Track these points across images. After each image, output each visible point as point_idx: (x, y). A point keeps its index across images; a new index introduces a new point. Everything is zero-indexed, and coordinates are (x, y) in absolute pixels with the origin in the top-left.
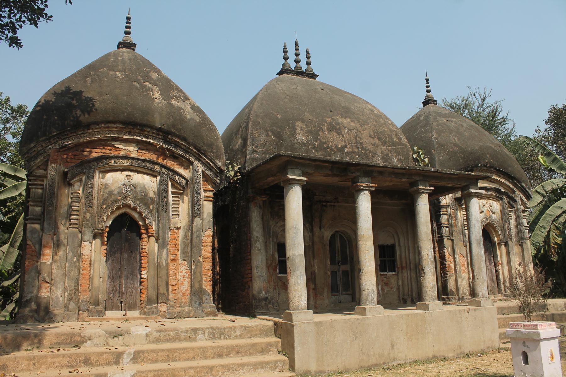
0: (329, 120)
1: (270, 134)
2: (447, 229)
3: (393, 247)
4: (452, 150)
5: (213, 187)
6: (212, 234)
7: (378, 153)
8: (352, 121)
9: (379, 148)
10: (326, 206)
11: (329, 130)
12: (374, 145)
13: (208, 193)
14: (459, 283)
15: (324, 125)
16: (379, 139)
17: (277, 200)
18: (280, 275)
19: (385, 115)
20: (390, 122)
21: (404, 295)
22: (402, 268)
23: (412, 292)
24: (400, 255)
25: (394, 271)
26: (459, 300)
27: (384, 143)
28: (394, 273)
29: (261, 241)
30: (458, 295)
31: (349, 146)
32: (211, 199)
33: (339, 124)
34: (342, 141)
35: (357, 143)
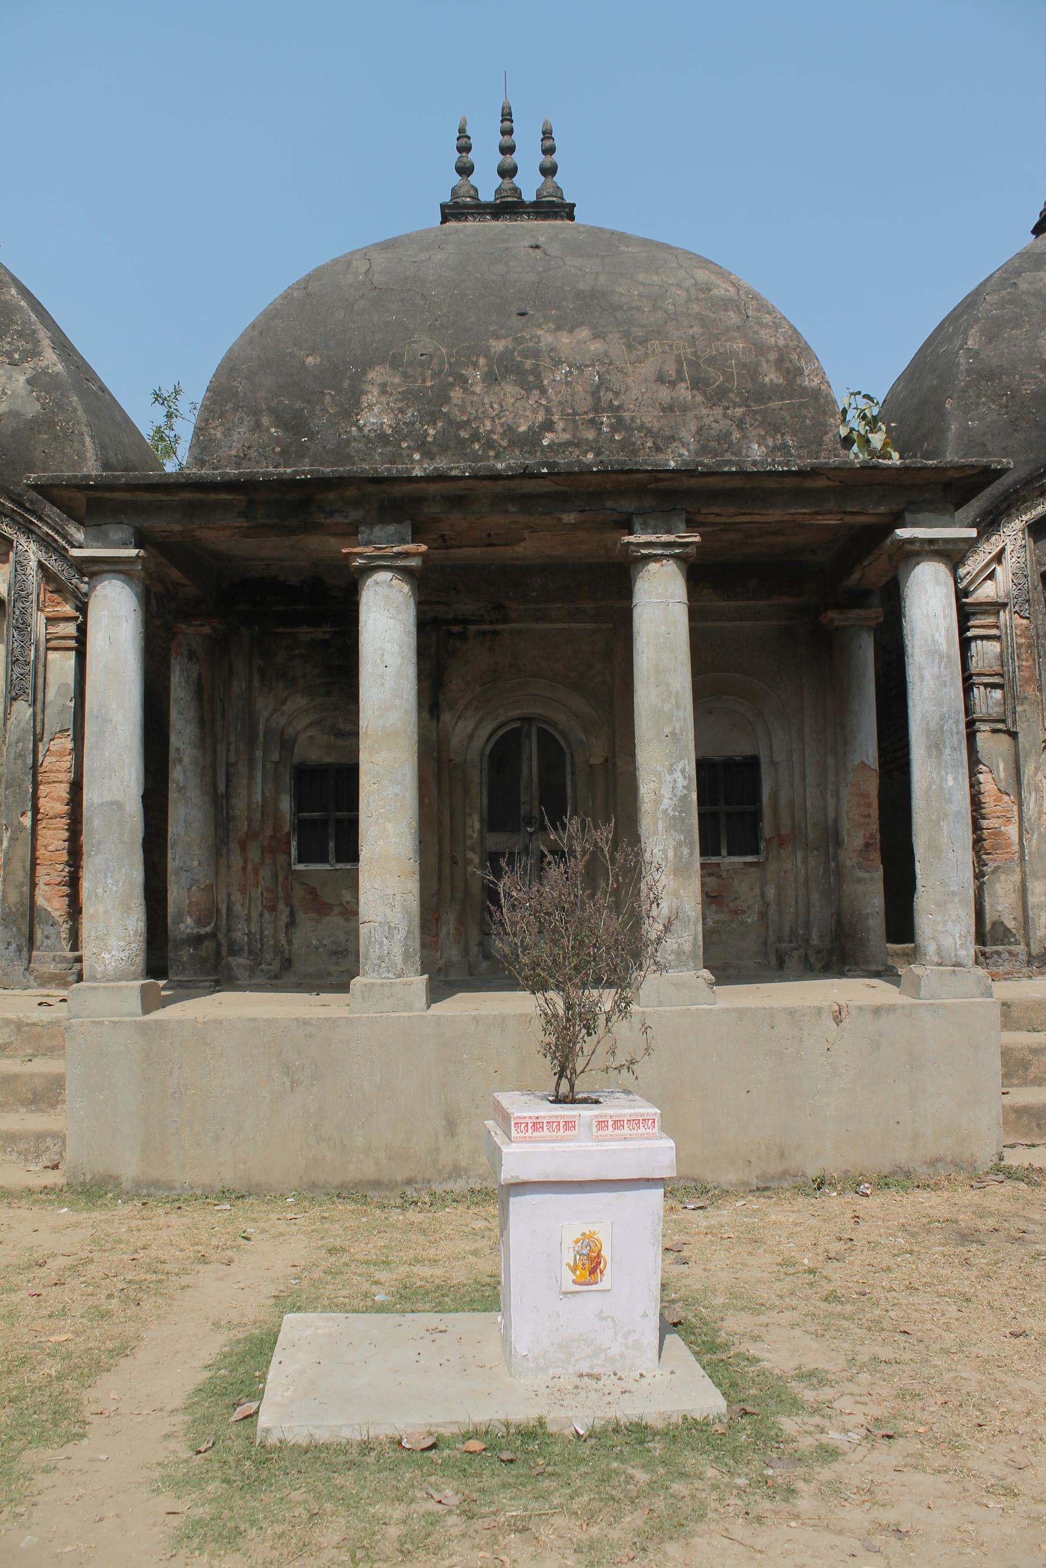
0: (498, 346)
1: (266, 420)
2: (997, 694)
3: (751, 765)
4: (1028, 388)
5: (77, 609)
6: (70, 745)
7: (683, 434)
8: (596, 336)
9: (690, 415)
10: (462, 636)
11: (491, 379)
12: (668, 409)
13: (62, 625)
14: (1032, 900)
15: (475, 365)
16: (696, 384)
17: (281, 630)
18: (300, 867)
19: (756, 297)
20: (768, 319)
21: (780, 940)
22: (782, 841)
23: (807, 925)
24: (775, 796)
25: (756, 852)
26: (1029, 963)
27: (717, 397)
28: (749, 859)
29: (186, 760)
30: (1028, 945)
31: (560, 425)
32: (72, 643)
33: (536, 354)
34: (535, 411)
35: (597, 409)
